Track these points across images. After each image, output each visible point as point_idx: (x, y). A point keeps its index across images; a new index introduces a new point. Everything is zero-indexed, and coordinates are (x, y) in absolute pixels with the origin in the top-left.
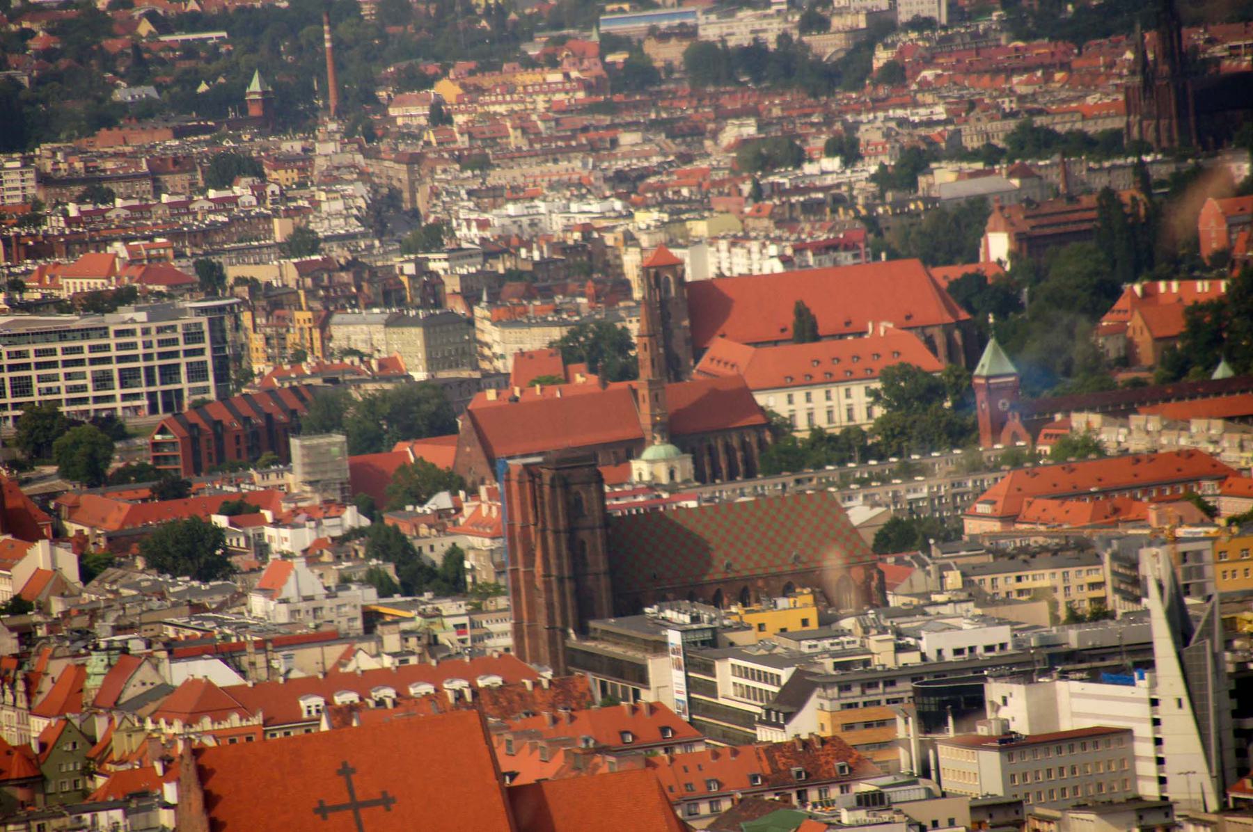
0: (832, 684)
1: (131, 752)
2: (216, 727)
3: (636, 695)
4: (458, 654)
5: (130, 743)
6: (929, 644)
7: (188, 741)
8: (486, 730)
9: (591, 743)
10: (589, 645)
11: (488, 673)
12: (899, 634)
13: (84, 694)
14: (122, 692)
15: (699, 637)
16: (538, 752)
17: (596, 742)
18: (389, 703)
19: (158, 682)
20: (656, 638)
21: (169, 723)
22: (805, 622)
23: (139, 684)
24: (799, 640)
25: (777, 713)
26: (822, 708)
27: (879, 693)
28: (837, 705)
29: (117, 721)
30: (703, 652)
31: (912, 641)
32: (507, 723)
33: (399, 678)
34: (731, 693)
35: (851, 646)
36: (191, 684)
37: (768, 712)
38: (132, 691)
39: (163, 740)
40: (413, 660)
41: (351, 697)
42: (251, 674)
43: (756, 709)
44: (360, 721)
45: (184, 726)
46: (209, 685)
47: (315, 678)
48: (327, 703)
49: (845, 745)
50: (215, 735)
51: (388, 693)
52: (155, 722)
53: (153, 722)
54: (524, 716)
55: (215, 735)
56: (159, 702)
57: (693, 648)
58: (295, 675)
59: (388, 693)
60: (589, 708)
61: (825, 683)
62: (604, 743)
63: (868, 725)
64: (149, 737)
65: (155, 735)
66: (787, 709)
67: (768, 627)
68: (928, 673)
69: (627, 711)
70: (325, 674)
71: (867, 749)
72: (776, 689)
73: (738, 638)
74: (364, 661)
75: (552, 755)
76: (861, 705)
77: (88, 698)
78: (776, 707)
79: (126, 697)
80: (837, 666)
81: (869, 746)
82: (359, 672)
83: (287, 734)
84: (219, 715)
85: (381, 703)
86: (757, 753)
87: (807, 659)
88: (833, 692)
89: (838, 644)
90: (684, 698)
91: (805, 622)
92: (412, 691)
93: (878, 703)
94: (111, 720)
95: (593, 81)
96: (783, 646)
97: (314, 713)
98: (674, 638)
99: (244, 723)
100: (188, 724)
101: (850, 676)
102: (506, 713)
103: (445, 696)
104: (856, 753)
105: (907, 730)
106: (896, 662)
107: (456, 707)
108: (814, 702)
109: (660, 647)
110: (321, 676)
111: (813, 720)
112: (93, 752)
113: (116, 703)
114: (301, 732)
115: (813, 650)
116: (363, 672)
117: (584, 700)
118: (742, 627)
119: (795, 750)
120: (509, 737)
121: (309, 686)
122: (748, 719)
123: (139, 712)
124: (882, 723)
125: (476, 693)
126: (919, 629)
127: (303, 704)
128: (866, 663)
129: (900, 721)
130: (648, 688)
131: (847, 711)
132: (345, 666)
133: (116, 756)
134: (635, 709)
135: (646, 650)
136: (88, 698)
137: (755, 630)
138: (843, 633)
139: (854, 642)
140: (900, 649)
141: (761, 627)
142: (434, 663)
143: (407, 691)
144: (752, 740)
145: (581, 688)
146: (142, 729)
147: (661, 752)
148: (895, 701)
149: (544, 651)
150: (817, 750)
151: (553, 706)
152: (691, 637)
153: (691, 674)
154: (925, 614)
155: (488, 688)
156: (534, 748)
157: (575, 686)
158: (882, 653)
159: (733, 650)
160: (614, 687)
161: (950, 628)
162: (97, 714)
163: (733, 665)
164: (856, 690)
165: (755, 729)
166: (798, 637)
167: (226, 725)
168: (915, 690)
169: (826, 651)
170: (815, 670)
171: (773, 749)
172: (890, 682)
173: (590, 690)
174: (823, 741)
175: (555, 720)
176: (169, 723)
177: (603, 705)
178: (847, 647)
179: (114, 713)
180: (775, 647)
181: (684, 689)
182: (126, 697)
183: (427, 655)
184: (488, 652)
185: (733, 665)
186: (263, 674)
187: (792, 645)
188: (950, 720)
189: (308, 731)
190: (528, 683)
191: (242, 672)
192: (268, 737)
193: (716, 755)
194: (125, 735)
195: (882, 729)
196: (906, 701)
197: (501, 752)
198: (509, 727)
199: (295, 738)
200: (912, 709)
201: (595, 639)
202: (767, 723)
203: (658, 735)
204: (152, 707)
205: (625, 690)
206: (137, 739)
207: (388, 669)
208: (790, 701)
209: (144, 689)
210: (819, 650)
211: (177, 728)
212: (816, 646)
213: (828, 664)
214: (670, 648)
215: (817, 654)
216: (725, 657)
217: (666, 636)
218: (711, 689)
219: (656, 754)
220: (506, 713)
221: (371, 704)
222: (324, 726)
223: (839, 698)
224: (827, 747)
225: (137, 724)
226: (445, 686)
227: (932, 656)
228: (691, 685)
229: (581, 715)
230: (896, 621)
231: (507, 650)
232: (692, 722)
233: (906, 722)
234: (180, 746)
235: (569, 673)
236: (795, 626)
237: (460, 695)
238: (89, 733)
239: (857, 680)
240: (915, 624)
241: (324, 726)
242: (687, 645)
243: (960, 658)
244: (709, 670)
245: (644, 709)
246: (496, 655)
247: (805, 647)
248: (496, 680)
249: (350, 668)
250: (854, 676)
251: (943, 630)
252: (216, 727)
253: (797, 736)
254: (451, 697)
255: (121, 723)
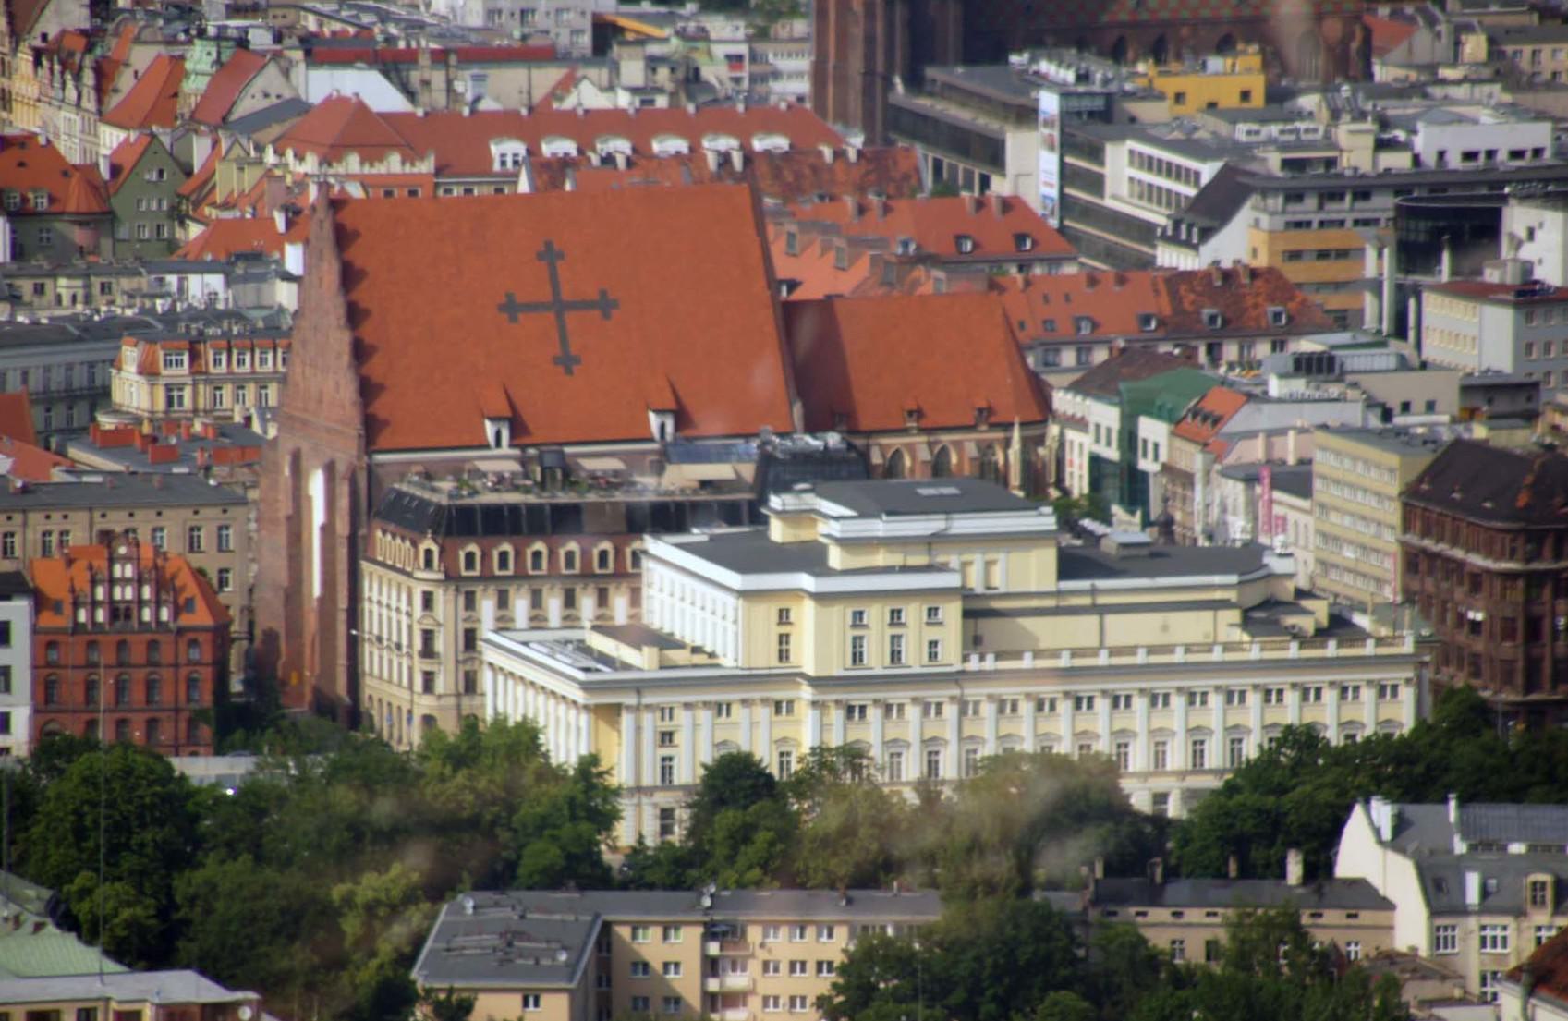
0: (1275, 191)
1: (242, 194)
2: (367, 169)
3: (985, 182)
4: (728, 98)
5: (240, 180)
6: (1426, 141)
7: (324, 186)
8: (759, 215)
9: (912, 247)
10: (923, 103)
11: (769, 129)
12: (1384, 123)
13: (180, 100)
14: (234, 103)
15: (1087, 104)
16: (832, 255)
17: (918, 247)
18: (621, 161)
19: (287, 94)
20: (1021, 100)
21: (300, 157)
22: (1245, 95)
23: (259, 96)
24: (1234, 122)
25: (1190, 227)
26: (1257, 223)
27: (1344, 208)
28: (1280, 222)
29: (224, 145)
30: (1089, 127)
31: (1401, 135)
32: (789, 208)
33: (639, 125)
34: (1124, 190)
35: (1310, 137)
36: (335, 103)
37: (1177, 224)
38: (249, 104)
39: (289, 180)
40: (661, 102)
41: (566, 147)
42: (424, 97)
43: (1158, 216)
44: (576, 184)
45: (320, 164)
46: (361, 107)
47: (517, 113)
48: (529, 152)
49: (1286, 283)
50: (365, 182)
51: (620, 146)
52: (279, 153)
53: (275, 152)
54: (816, 200)
55: (365, 182)
56: (287, 125)
57: (1075, 121)
58: (487, 105)
59: (620, 146)
60: (913, 195)
61: (1267, 188)
62: (932, 250)
63: (1323, 255)
64: (269, 174)
65: (278, 172)
66: (1206, 223)
67: (1189, 98)
68: (1420, 185)
69: (970, 206)
70: (531, 109)
71: (1318, 290)
72: (1191, 192)
73: (1147, 111)
74: (588, 96)
75: (854, 259)
76: (1315, 225)
77: (186, 105)
78: (1189, 218)
79: (238, 112)
80: (1287, 164)
81: (1321, 286)
82: (580, 112)
83: (469, 191)
84: (372, 153)
85: (608, 160)
86: (1154, 284)
87: (1245, 150)
88: (1277, 202)
89: (1291, 132)
90: (1054, 193)
91: (1245, 95)
92: (656, 147)
93: (1342, 223)
94: (215, 143)
95: (177, 774)
96: (1209, 128)
97: (510, 165)
98: (1049, 103)
99: (408, 169)
100: (326, 161)
101: (1305, 179)
102: (791, 192)
103: (704, 158)
104: (1300, 295)
105: (1380, 267)
106: (1375, 162)
107: (717, 177)
108: (1245, 215)
109: (1026, 115)
110: (524, 112)
111: (1241, 241)
112: (188, 186)
113: (224, 119)
114: (488, 191)
115: (1254, 138)
116: (587, 111)
117: (908, 184)
118: (1150, 94)
119: (1210, 283)
120: (793, 228)
121: (506, 124)
122: (1145, 231)
123: (256, 136)
124: (1343, 254)
125: (749, 157)
126: (1416, 117)
127: (495, 150)
128: (1331, 163)
129: (1371, 254)
130: (1004, 175)
131: (1294, 233)
132: (561, 99)
133: (219, 197)
134: (980, 204)
135: (1006, 119)
136: (186, 105)
137: (1169, 102)
138: (1300, 115)
139: (1315, 130)
140: (1382, 145)
141: (1179, 97)
142: (691, 108)
143: (650, 148)
144: (1148, 263)
145: (904, 166)
146: (260, 162)
147: (1013, 270)
148: (1366, 223)
149: (855, 103)
150: (1244, 286)
151: (861, 189)
152: (1075, 104)
153: (1069, 159)
154: (1425, 96)
155: (767, 154)
156: (826, 248)
157: (895, 163)
158: (1355, 149)
159: (1132, 127)
160: (953, 169)
161: (1461, 119)
162: (196, 132)
163: (1132, 152)
164: (1311, 202)
165: (1154, 247)
166: (1233, 117)
167: (380, 169)
168: (1398, 208)
169: (1271, 141)
170: (1254, 167)
171: (1178, 279)
172: (1363, 194)
173: (917, 171)
174: (1254, 273)
175: (862, 210)
176: (300, 157)
177: (936, 194)
178: (1304, 137)
179: (220, 133)
180: (1196, 129)
181: (1055, 179)
182: (238, 112)
183: (683, 97)
184: (773, 99)
185: (1132, 152)
186: (440, 99)
187: (1223, 128)
188: (1446, 257)
189: (499, 191)
190: (827, 152)
191: (410, 94)
192: (441, 192)
193: (1093, 280)
194: (234, 166)
195: (1342, 264)
196: (1383, 223)
197: (778, 249)
198: (793, 215)
199: (481, 199)
200: (1390, 235)
201: (931, 94)
202: (1174, 240)
203: (1011, 245)
204: (276, 130)
205: (969, 176)
206: (251, 176)
207: (624, 112)
208: (1212, 209)
209: (264, 104)
210: (1263, 137)
211: (310, 164)
212: (1257, 133)
213: (1274, 160)
214: (1041, 118)
215: (1258, 145)
216: (1121, 138)
217: (1037, 100)
218: (1096, 184)
219: (1006, 273)
220: (791, 192)
221: (595, 160)
222: (524, 186)
223: (1284, 212)
224: (1259, 283)
225: (253, 153)
226: (706, 144)
227: (1430, 160)
228: (1066, 175)
229: (901, 205)
230: (1381, 104)
231: (801, 99)
232: (1062, 230)
233: (1380, 255)
234: (313, 192)
235: (889, 143)
236: (1230, 100)
237: (725, 159)
238: (183, 159)
239: (1313, 189)
240: (1410, 111)
241: (524, 186)
242: (1066, 115)
243: (1471, 165)
244: (1096, 154)
245: (995, 206)
246: (783, 106)
247: (1241, 131)
248: (780, 143)
249: (569, 103)
250: (1313, 180)
251: (1451, 122)
252: (367, 169)
253: (1216, 263)
254: (712, 161)
255: (228, 152)
